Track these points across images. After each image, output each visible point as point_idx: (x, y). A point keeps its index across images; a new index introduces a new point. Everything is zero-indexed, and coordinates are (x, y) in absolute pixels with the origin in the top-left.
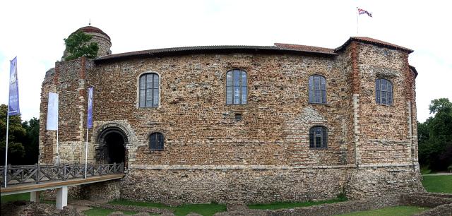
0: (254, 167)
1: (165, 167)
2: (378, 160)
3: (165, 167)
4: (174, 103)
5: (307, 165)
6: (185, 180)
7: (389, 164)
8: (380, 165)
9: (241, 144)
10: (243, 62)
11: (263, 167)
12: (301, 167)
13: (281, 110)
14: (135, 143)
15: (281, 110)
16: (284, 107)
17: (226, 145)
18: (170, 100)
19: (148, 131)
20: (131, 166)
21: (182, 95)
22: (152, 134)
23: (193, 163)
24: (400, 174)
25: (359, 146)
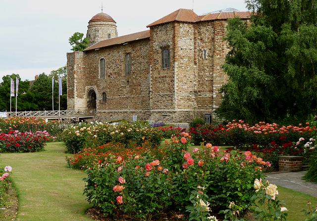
0: (131, 111)
1: (107, 111)
2: (158, 107)
3: (107, 111)
4: (109, 76)
5: (148, 109)
6: (111, 117)
7: (162, 110)
8: (159, 110)
9: (127, 98)
10: (129, 50)
11: (134, 110)
12: (146, 111)
13: (140, 77)
14: (99, 97)
15: (140, 77)
16: (142, 75)
17: (123, 98)
18: (109, 74)
19: (102, 91)
20: (98, 111)
21: (111, 72)
22: (104, 93)
23: (114, 108)
24: (167, 117)
25: (151, 98)
